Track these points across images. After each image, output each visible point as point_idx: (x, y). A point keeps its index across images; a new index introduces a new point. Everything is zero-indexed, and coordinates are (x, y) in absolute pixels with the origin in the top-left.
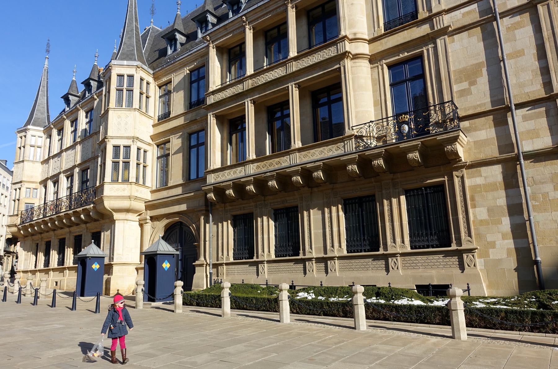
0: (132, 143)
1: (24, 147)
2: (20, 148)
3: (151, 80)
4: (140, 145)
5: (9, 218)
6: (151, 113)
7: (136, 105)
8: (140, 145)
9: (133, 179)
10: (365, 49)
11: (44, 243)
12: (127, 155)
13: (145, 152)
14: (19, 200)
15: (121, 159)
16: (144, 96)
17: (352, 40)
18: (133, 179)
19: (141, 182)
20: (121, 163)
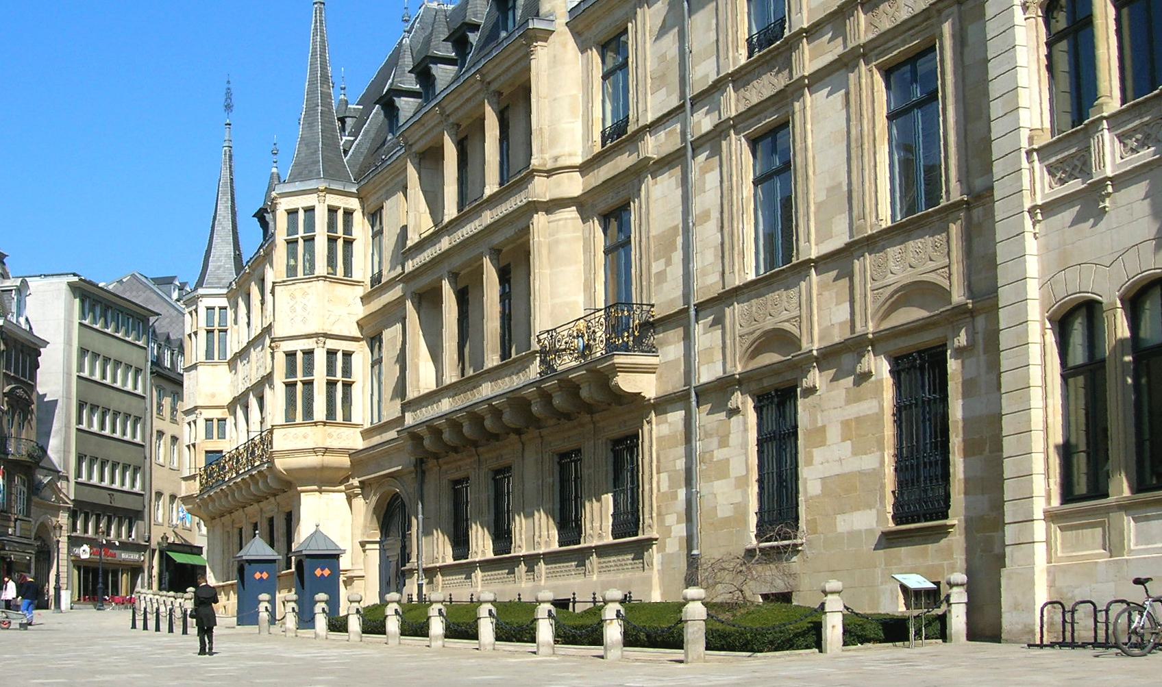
0: (315, 346)
1: (196, 333)
2: (190, 336)
3: (354, 203)
4: (332, 344)
5: (183, 483)
6: (357, 274)
7: (321, 267)
8: (332, 344)
9: (320, 412)
10: (573, 185)
11: (236, 531)
12: (309, 367)
13: (347, 355)
14: (194, 445)
15: (300, 376)
16: (340, 243)
17: (550, 173)
18: (320, 412)
19: (339, 418)
20: (299, 386)
